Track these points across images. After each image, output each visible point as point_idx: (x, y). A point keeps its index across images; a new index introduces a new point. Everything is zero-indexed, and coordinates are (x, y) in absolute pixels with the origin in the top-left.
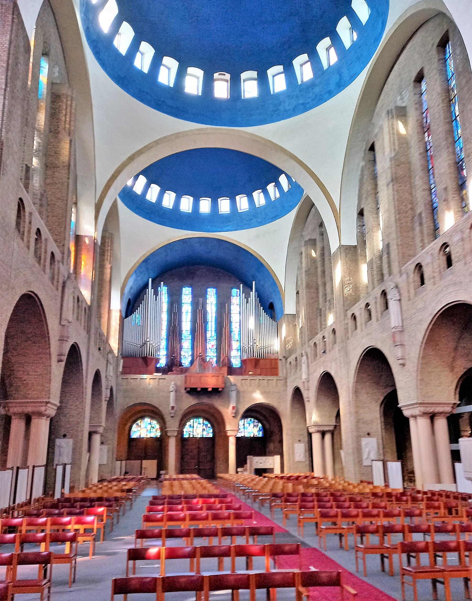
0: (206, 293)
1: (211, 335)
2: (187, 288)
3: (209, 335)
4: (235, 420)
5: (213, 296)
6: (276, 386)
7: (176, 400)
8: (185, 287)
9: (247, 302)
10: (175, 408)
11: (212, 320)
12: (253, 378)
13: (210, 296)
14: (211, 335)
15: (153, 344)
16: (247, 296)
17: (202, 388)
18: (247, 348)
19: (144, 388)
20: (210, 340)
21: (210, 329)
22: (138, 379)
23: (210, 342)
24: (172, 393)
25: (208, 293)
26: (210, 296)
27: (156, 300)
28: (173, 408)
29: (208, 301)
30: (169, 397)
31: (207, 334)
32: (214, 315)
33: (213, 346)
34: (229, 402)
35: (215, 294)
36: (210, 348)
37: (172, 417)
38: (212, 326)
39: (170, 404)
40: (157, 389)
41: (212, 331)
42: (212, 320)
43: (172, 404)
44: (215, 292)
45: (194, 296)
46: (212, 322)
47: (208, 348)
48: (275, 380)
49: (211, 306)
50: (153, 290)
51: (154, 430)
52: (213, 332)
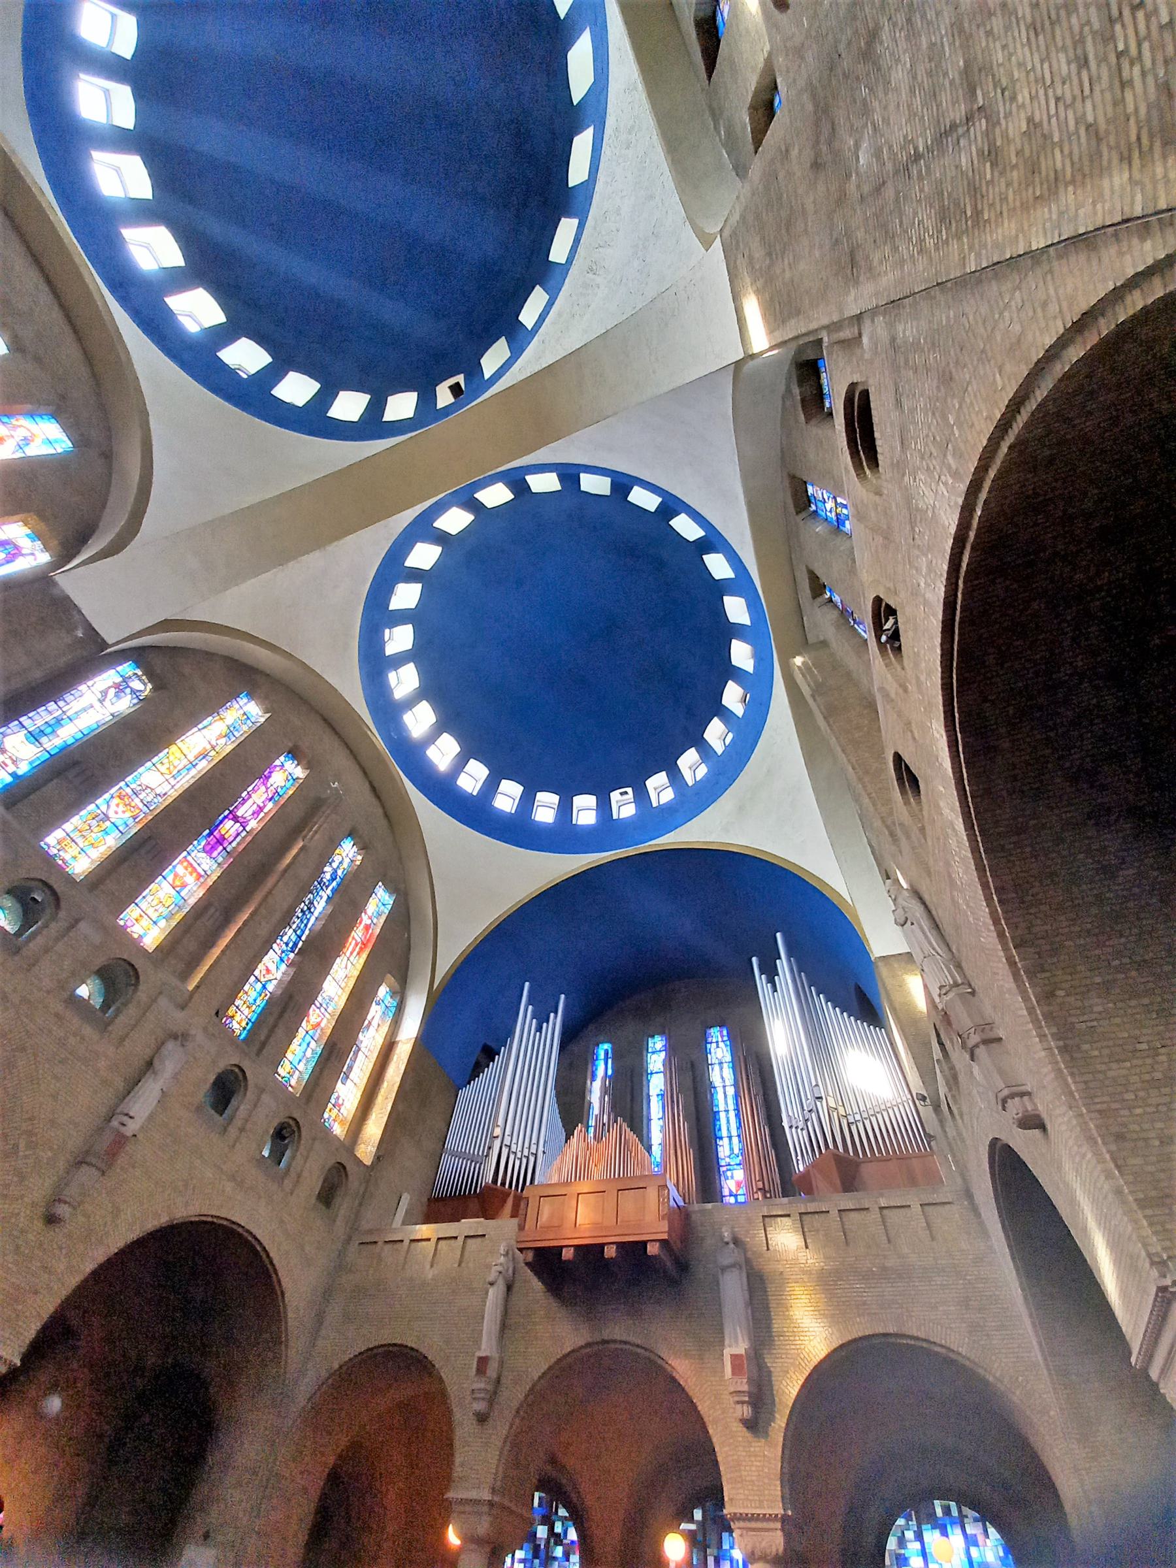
0: (704, 1040)
1: (731, 1149)
2: (657, 1038)
3: (724, 1150)
4: (758, 1445)
5: (721, 1044)
6: (933, 1238)
8: (653, 1036)
9: (775, 990)
10: (492, 1372)
12: (812, 1207)
13: (714, 1045)
14: (731, 1149)
15: (513, 1148)
16: (771, 972)
18: (801, 1124)
21: (724, 1133)
22: (406, 1242)
23: (729, 1173)
24: (492, 1291)
25: (709, 1040)
26: (714, 1045)
27: (539, 1029)
29: (712, 1058)
31: (720, 1149)
32: (731, 1091)
35: (726, 1038)
39: (480, 1349)
41: (730, 1137)
43: (487, 1346)
44: (725, 1033)
45: (671, 1050)
46: (727, 1111)
47: (726, 1192)
48: (916, 1208)
49: (721, 1069)
52: (735, 1140)
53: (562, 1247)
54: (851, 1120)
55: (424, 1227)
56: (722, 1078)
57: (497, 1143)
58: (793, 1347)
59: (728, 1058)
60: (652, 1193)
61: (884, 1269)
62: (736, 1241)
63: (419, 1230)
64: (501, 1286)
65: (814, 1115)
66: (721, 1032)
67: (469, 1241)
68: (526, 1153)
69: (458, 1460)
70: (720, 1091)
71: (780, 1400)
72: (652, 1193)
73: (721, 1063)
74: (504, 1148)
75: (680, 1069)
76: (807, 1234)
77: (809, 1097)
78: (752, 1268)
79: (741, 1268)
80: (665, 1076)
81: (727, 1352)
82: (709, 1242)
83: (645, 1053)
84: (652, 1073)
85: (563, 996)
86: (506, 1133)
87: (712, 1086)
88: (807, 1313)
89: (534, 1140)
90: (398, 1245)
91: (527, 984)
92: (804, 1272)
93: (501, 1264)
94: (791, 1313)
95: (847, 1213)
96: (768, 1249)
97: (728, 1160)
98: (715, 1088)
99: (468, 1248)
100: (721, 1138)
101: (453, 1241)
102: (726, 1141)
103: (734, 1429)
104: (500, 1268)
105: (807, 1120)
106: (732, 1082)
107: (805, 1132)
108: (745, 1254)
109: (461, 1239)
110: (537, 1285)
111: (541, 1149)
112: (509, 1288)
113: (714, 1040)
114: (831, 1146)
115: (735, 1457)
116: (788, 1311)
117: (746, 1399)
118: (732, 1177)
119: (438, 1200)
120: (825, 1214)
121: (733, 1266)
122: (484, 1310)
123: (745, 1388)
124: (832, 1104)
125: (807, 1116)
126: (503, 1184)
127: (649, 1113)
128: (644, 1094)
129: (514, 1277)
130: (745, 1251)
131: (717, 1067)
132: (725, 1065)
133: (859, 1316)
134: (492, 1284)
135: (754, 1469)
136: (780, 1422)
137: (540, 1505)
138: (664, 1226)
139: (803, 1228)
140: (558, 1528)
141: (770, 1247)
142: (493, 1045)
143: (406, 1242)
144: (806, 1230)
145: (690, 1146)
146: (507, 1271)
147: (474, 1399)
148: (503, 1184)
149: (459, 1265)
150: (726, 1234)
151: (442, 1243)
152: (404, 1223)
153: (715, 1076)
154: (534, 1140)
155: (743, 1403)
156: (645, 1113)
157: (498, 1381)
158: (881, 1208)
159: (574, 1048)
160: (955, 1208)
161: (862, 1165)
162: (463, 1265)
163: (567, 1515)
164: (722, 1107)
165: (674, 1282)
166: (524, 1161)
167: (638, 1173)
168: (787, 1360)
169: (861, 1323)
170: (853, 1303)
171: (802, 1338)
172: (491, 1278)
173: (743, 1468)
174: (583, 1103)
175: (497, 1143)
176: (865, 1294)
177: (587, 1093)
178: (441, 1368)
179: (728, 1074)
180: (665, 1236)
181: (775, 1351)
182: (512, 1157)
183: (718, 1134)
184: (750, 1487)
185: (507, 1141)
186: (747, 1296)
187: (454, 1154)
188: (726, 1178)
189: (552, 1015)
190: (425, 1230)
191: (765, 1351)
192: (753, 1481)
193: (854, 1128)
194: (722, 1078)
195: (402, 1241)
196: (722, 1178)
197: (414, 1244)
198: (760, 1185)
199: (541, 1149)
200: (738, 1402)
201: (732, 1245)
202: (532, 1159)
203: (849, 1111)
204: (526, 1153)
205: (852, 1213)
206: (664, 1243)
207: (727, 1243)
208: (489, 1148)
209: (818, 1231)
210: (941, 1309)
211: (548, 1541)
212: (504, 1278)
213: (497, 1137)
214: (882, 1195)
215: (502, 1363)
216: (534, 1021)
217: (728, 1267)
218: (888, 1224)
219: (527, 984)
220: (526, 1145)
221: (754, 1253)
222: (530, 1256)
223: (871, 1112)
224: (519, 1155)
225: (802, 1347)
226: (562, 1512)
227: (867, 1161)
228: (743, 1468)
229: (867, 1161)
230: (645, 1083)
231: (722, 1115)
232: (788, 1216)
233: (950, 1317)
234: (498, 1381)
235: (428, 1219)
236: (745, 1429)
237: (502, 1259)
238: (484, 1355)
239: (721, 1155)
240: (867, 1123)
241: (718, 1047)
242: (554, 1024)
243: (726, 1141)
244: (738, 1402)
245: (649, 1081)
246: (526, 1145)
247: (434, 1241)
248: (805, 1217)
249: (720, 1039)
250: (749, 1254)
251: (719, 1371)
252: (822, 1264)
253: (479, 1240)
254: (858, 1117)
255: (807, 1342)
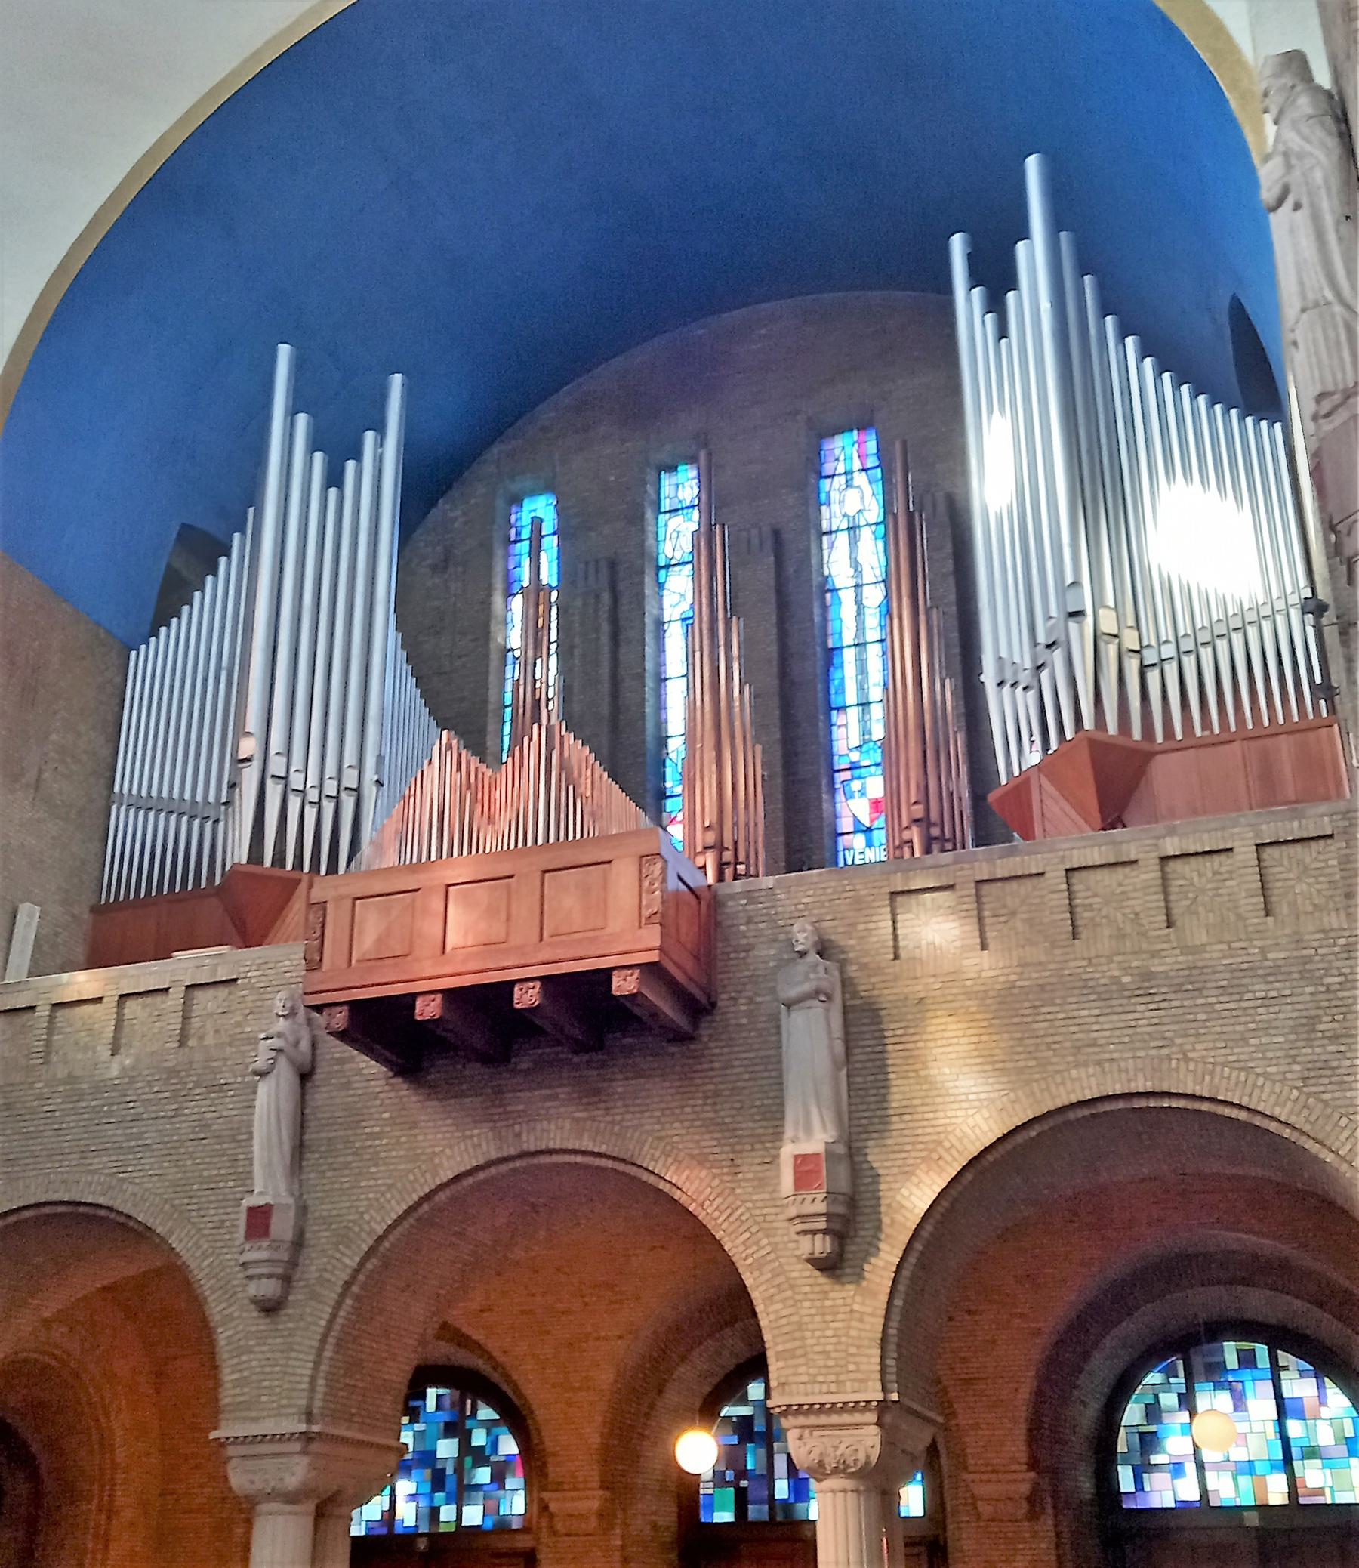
0: (814, 469)
4: (842, 1295)
5: (860, 479)
7: (300, 1149)
8: (672, 469)
10: (282, 1227)
11: (861, 627)
17: (451, 995)
18: (1025, 678)
19: (71, 1079)
20: (854, 767)
21: (851, 697)
23: (856, 785)
25: (828, 469)
27: (334, 478)
28: (259, 1220)
29: (832, 517)
30: (241, 1135)
31: (838, 733)
32: (874, 596)
33: (876, 805)
34: (773, 1118)
35: (872, 462)
36: (860, 828)
37: (270, 1308)
38: (862, 670)
40: (173, 1072)
42: (861, 627)
44: (871, 446)
46: (860, 645)
48: (1245, 853)
49: (853, 543)
50: (302, 419)
51: (483, 1475)
53: (414, 996)
54: (1150, 657)
55: (82, 976)
56: (856, 567)
57: (250, 777)
58: (930, 1130)
59: (874, 511)
60: (624, 875)
61: (1148, 976)
62: (824, 949)
63: (68, 984)
64: (285, 1076)
65: (1058, 655)
66: (861, 443)
67: (199, 995)
68: (330, 788)
69: (228, 1376)
70: (847, 597)
71: (893, 1221)
72: (624, 875)
73: (853, 529)
74: (269, 782)
75: (739, 555)
76: (988, 921)
77: (1054, 613)
78: (855, 994)
79: (829, 997)
80: (696, 577)
81: (788, 1151)
82: (765, 952)
83: (649, 515)
84: (667, 567)
85: (397, 380)
86: (273, 750)
87: (825, 588)
88: (966, 1069)
89: (350, 758)
90: (25, 1016)
91: (284, 351)
92: (969, 995)
93: (279, 1035)
94: (932, 1072)
95: (1084, 874)
96: (896, 957)
97: (855, 756)
98: (834, 590)
99: (197, 1010)
100: (842, 709)
101: (158, 999)
102: (853, 714)
103: (795, 1274)
104: (275, 1043)
105: (1039, 668)
106: (880, 574)
107: (1032, 694)
108: (842, 972)
109: (177, 995)
110: (368, 1067)
111: (370, 775)
112: (305, 1076)
113: (841, 469)
114: (1088, 723)
115: (795, 1319)
116: (927, 1068)
117: (823, 1226)
118: (862, 793)
119: (116, 906)
120: (1035, 880)
121: (816, 994)
122: (250, 1124)
123: (821, 1207)
124: (1108, 625)
125: (1044, 656)
126: (279, 859)
127: (660, 664)
128: (648, 620)
129: (313, 1054)
130: (842, 965)
131: (842, 539)
132: (866, 534)
133: (1077, 1066)
134: (263, 1074)
135: (829, 1333)
136: (888, 1256)
137: (438, 1408)
138: (652, 936)
139: (980, 910)
140: (479, 1438)
141: (903, 953)
142: (211, 525)
143: (44, 1011)
144: (986, 913)
145: (757, 739)
146: (297, 1043)
147: (250, 1278)
148: (279, 859)
149: (182, 1043)
150: (801, 937)
151: (132, 1007)
152: (36, 970)
153: (837, 563)
154: (350, 758)
155: (814, 1232)
156: (649, 665)
157: (299, 1243)
158: (1165, 859)
159: (449, 510)
160: (1333, 846)
161: (1159, 759)
162: (192, 1042)
163: (498, 1417)
164: (848, 638)
165: (681, 1038)
166: (329, 808)
167: (591, 831)
168: (913, 1154)
169: (1079, 1079)
170: (1068, 1044)
171: (949, 1114)
172: (261, 1064)
173: (808, 1334)
174: (487, 656)
175: (250, 777)
176: (1096, 1027)
177: (494, 627)
178: (171, 1232)
179: (872, 553)
180: (653, 957)
181: (889, 1142)
182: (294, 803)
183: (835, 701)
184: (821, 1363)
185: (277, 766)
186: (839, 1047)
187: (141, 804)
188: (849, 796)
189: (370, 436)
190: (83, 982)
191: (871, 1143)
192: (828, 1353)
193: (1153, 677)
194: (856, 567)
195: (32, 1008)
196: (840, 797)
197: (61, 1013)
198: (918, 811)
199: (370, 775)
200: (805, 1232)
201: (813, 957)
202: (348, 803)
203: (1150, 639)
204: (330, 788)
205: (1099, 871)
206: (652, 971)
207: (802, 954)
208: (232, 786)
209: (1013, 913)
210: (1252, 1041)
211: (459, 1462)
212: (292, 1061)
213: (248, 760)
214: (1172, 832)
215: (303, 1210)
216: (318, 456)
217: (799, 1000)
218: (1173, 890)
219: (284, 351)
220: (331, 769)
221: (864, 967)
222: (340, 1019)
223: (1204, 637)
224: (313, 795)
225: (949, 1129)
226: (486, 1413)
227: (1173, 747)
228: (808, 1334)
229: (1173, 747)
230: (648, 591)
231: (849, 656)
232: (950, 887)
233: (1270, 1055)
234: (299, 1243)
235: (96, 960)
236: (818, 1273)
237: (282, 1025)
238: (259, 1201)
239: (840, 746)
240: (1189, 663)
241: (849, 485)
242: (379, 460)
243: (853, 714)
244: (805, 1232)
245: (661, 586)
246: (331, 769)
247: (110, 1002)
248: (986, 889)
249: (857, 465)
250: (852, 970)
251: (766, 1183)
252: (1013, 977)
253: (222, 992)
254: (1168, 651)
255: (959, 1121)
